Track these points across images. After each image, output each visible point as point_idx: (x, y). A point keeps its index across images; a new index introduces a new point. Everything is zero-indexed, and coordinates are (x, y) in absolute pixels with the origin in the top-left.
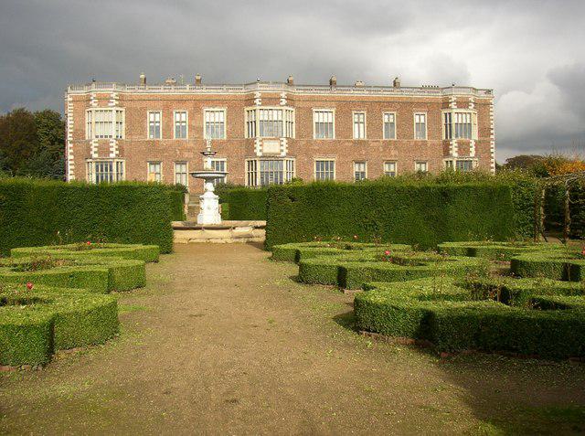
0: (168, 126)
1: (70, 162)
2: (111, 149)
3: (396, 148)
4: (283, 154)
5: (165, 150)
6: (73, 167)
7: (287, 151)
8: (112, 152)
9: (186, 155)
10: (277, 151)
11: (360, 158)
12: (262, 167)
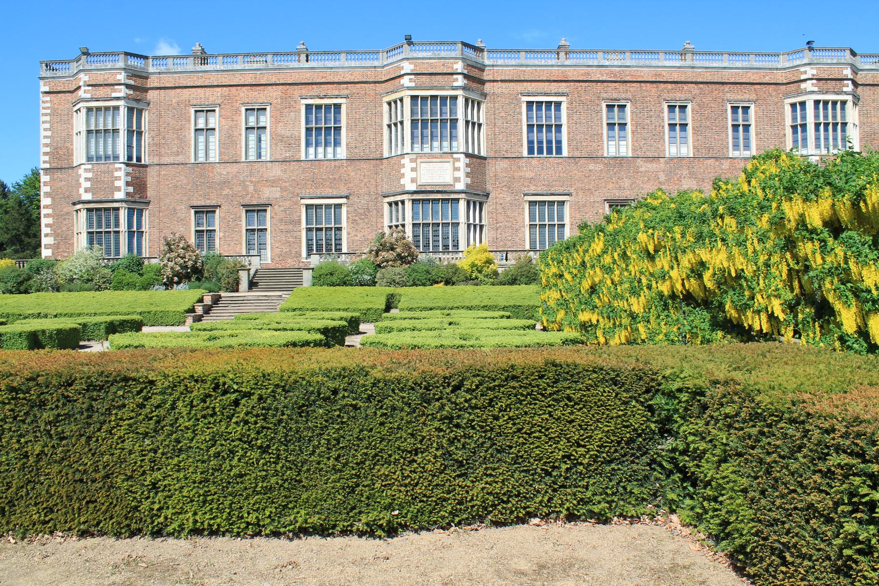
0: (230, 136)
1: (44, 212)
2: (117, 184)
3: (692, 175)
4: (460, 186)
5: (226, 183)
6: (50, 221)
7: (469, 181)
8: (118, 189)
9: (267, 194)
10: (448, 180)
11: (618, 195)
12: (415, 215)
